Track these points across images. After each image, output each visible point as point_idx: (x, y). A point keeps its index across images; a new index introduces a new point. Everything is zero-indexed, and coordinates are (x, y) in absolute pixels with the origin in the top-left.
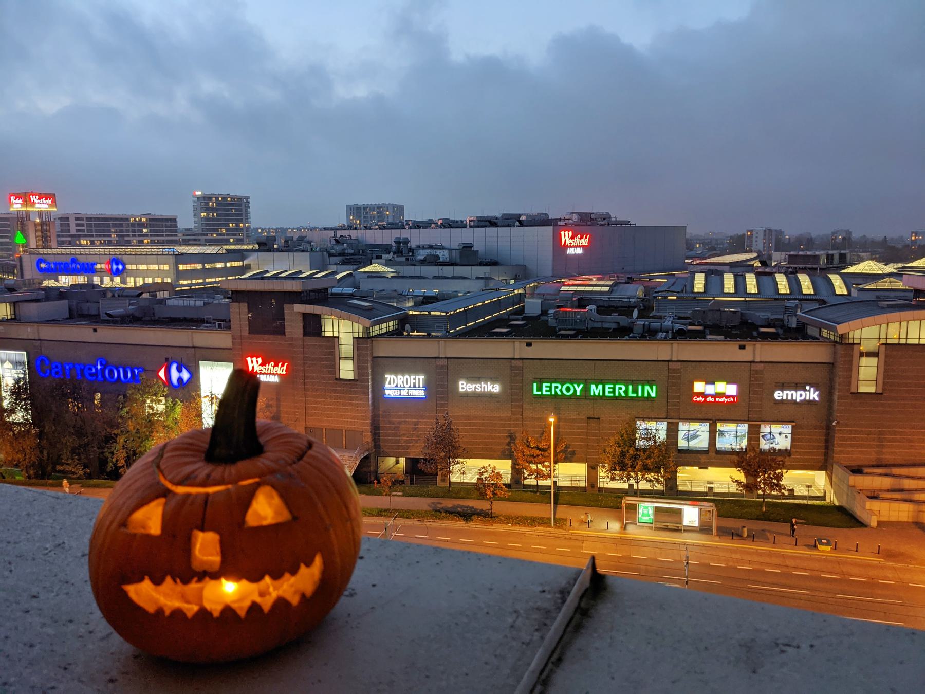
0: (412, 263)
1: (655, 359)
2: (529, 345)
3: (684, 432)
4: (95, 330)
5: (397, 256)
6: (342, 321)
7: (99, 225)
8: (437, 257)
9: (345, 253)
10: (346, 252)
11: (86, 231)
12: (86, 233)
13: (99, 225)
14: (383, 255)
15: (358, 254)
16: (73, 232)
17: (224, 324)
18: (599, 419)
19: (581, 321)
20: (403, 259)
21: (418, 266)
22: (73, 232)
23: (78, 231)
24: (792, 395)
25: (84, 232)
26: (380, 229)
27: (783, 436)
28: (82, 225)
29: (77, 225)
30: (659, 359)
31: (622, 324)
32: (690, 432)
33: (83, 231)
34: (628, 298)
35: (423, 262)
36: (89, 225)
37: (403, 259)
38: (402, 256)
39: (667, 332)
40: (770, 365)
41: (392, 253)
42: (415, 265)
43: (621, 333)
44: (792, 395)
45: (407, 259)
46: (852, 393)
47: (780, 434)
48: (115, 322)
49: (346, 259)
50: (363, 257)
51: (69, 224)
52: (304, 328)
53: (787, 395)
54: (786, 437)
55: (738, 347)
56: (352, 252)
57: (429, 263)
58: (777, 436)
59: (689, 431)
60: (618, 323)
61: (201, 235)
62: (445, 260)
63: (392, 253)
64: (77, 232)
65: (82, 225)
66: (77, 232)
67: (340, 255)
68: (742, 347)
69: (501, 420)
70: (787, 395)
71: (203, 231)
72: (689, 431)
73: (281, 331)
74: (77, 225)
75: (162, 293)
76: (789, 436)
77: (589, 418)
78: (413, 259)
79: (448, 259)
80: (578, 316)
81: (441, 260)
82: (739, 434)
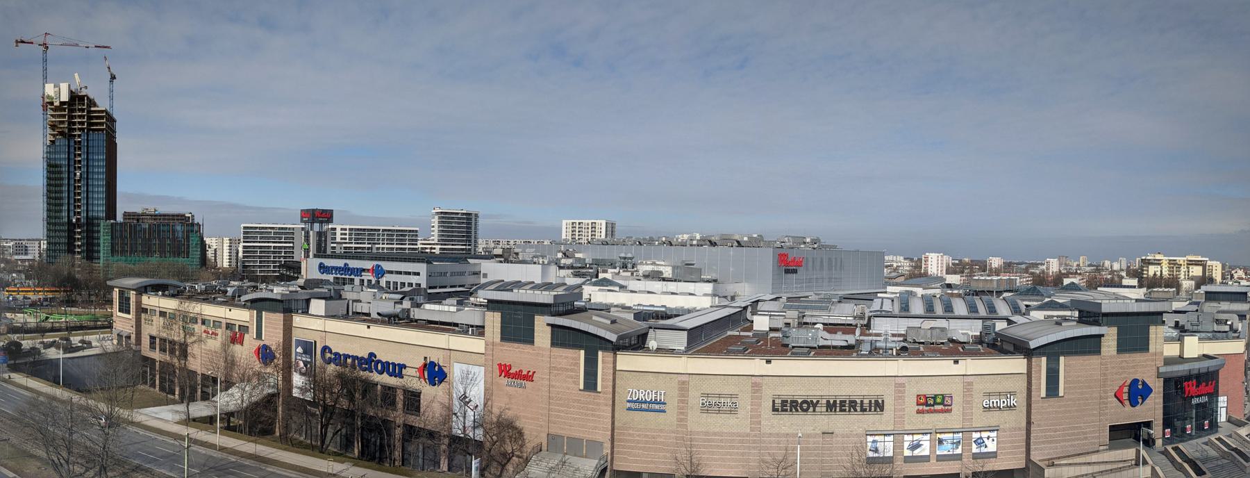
0: (637, 278)
1: (884, 375)
2: (769, 362)
3: (908, 443)
6: (758, 308)
7: (358, 234)
8: (661, 273)
12: (347, 241)
13: (358, 234)
16: (338, 240)
17: (479, 330)
18: (833, 433)
19: (812, 338)
20: (629, 274)
22: (338, 240)
23: (341, 239)
24: (997, 402)
26: (603, 244)
27: (991, 439)
28: (345, 234)
29: (342, 234)
30: (887, 375)
31: (849, 343)
32: (914, 442)
33: (345, 239)
34: (846, 317)
35: (647, 276)
36: (350, 234)
37: (629, 274)
38: (627, 271)
39: (892, 349)
40: (979, 377)
41: (618, 268)
42: (640, 280)
43: (848, 351)
44: (997, 402)
45: (632, 274)
46: (1042, 398)
47: (988, 438)
51: (335, 233)
52: (552, 339)
53: (993, 402)
54: (993, 440)
55: (953, 361)
58: (985, 440)
59: (913, 441)
60: (847, 341)
61: (437, 244)
63: (618, 268)
65: (345, 234)
67: (571, 267)
68: (956, 362)
69: (740, 436)
70: (993, 402)
71: (439, 241)
72: (913, 441)
73: (530, 340)
74: (342, 234)
76: (995, 439)
77: (823, 433)
80: (810, 335)
81: (664, 276)
82: (955, 441)
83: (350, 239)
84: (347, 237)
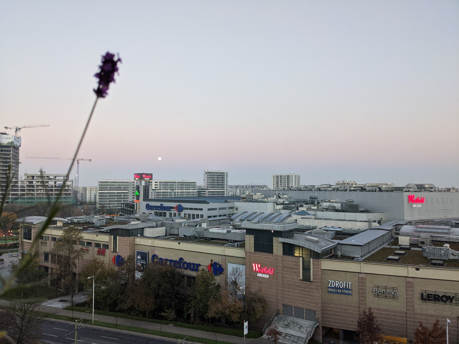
4: (179, 243)
5: (313, 206)
9: (284, 203)
10: (285, 203)
11: (159, 187)
12: (158, 189)
14: (304, 205)
15: (291, 204)
21: (324, 211)
23: (156, 187)
25: (158, 188)
33: (157, 187)
35: (327, 209)
37: (316, 208)
45: (318, 208)
48: (187, 240)
49: (285, 206)
50: (293, 205)
56: (288, 203)
57: (330, 210)
62: (339, 209)
64: (155, 188)
66: (155, 188)
67: (282, 204)
75: (204, 223)
78: (321, 208)
79: (340, 208)
83: (160, 187)
84: (158, 186)
